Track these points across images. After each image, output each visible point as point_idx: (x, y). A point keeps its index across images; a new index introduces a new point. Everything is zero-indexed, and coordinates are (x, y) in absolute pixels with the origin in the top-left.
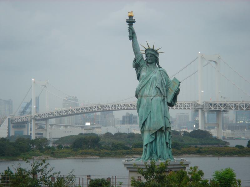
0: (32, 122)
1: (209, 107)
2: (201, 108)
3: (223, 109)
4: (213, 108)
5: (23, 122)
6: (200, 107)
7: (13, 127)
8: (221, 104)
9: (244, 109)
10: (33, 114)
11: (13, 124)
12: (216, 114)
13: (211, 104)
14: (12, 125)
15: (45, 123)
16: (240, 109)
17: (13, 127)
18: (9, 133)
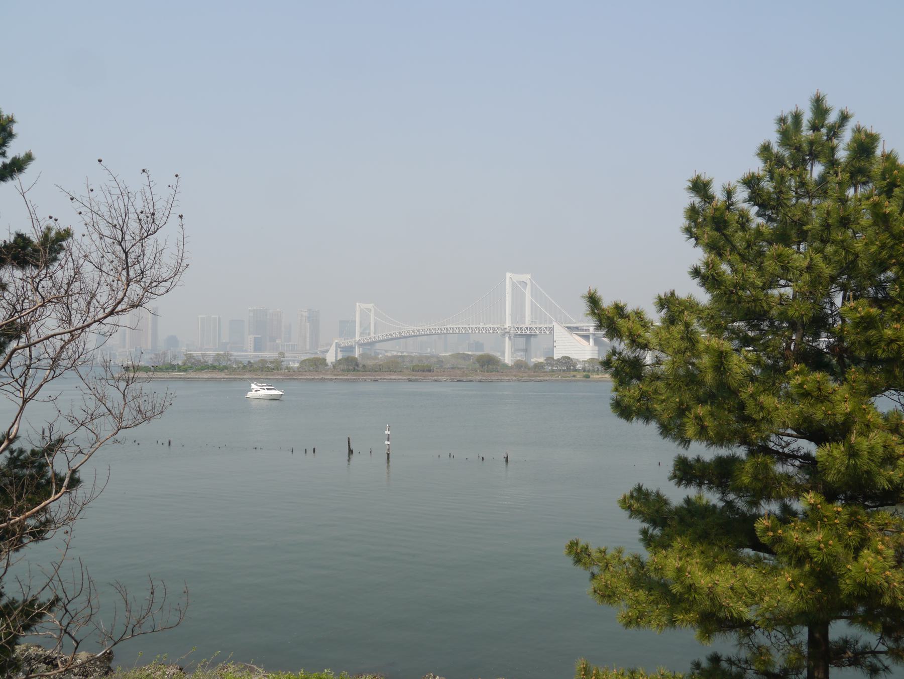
0: (356, 347)
1: (516, 330)
2: (509, 332)
3: (528, 332)
4: (519, 332)
5: (350, 346)
6: (507, 331)
7: (341, 351)
8: (527, 328)
9: (548, 332)
10: (357, 338)
11: (341, 348)
12: (525, 339)
13: (518, 328)
14: (339, 350)
15: (369, 347)
16: (544, 333)
17: (341, 351)
18: (336, 357)
